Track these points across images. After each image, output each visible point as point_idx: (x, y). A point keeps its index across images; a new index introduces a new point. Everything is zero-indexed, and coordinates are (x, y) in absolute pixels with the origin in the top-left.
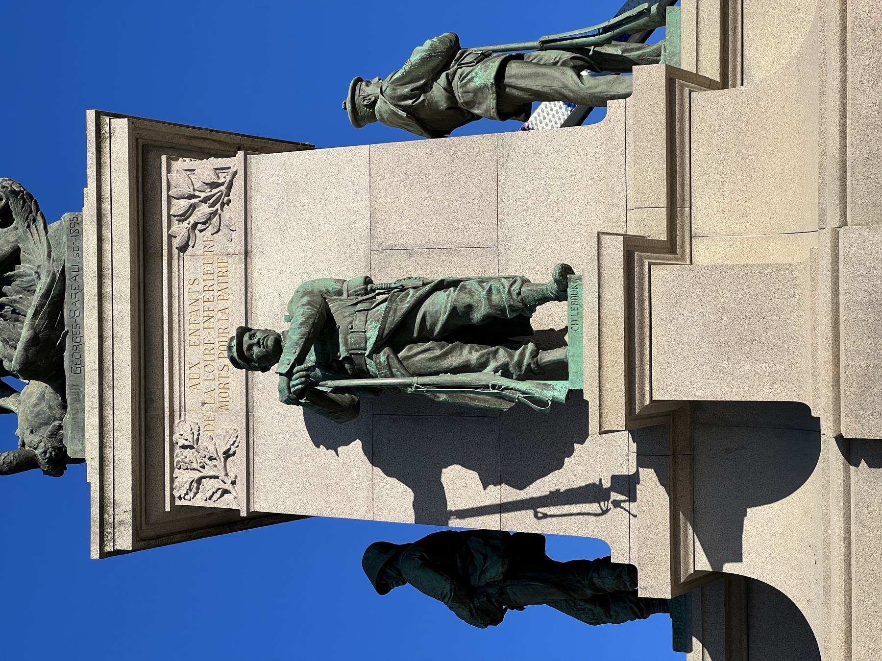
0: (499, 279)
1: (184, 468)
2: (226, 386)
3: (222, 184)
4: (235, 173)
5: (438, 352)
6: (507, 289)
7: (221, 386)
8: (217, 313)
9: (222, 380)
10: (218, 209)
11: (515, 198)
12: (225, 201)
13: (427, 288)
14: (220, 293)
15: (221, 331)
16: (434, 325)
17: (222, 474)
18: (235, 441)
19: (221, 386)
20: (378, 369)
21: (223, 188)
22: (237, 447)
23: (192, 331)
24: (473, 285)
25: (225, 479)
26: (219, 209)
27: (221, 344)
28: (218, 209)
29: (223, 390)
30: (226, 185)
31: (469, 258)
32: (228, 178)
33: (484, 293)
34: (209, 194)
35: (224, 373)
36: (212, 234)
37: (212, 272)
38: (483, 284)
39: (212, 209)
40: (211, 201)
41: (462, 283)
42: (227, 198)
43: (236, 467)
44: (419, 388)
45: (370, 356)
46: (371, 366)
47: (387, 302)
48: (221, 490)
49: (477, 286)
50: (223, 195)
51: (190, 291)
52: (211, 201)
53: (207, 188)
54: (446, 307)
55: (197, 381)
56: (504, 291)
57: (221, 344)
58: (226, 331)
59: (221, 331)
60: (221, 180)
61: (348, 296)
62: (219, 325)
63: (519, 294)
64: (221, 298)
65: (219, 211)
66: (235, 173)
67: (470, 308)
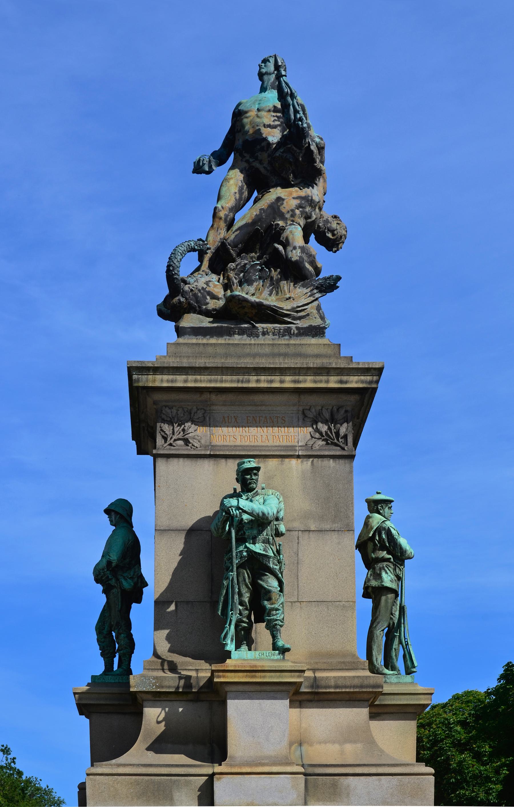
0: (283, 613)
1: (178, 412)
2: (225, 440)
3: (338, 440)
4: (343, 449)
5: (247, 580)
6: (278, 618)
7: (225, 437)
8: (266, 434)
9: (228, 438)
10: (324, 437)
11: (323, 611)
12: (329, 441)
13: (280, 575)
14: (277, 437)
15: (256, 437)
16: (263, 581)
17: (175, 437)
18: (194, 446)
19: (225, 437)
20: (240, 551)
21: (336, 441)
22: (191, 448)
23: (255, 418)
24: (282, 600)
25: (173, 440)
26: (324, 438)
27: (249, 437)
28: (324, 437)
29: (222, 438)
30: (337, 442)
31: (293, 586)
32: (341, 444)
33: (277, 607)
34: (333, 431)
35: (232, 438)
36: (310, 432)
37: (289, 432)
38: (281, 606)
39: (324, 433)
40: (329, 432)
41: (282, 594)
42: (330, 443)
43: (180, 447)
44: (231, 576)
45: (246, 547)
46: (241, 548)
47: (274, 556)
48: (166, 436)
49: (280, 602)
50: (332, 441)
51: (279, 418)
52: (329, 432)
53: (336, 430)
54: (270, 587)
55: (227, 421)
56: (277, 617)
57: (249, 437)
58: (256, 440)
59: (256, 437)
60: (340, 440)
61: (276, 525)
62: (259, 436)
63: (276, 624)
64: (274, 438)
65: (323, 438)
66: (343, 449)
67: (269, 599)
